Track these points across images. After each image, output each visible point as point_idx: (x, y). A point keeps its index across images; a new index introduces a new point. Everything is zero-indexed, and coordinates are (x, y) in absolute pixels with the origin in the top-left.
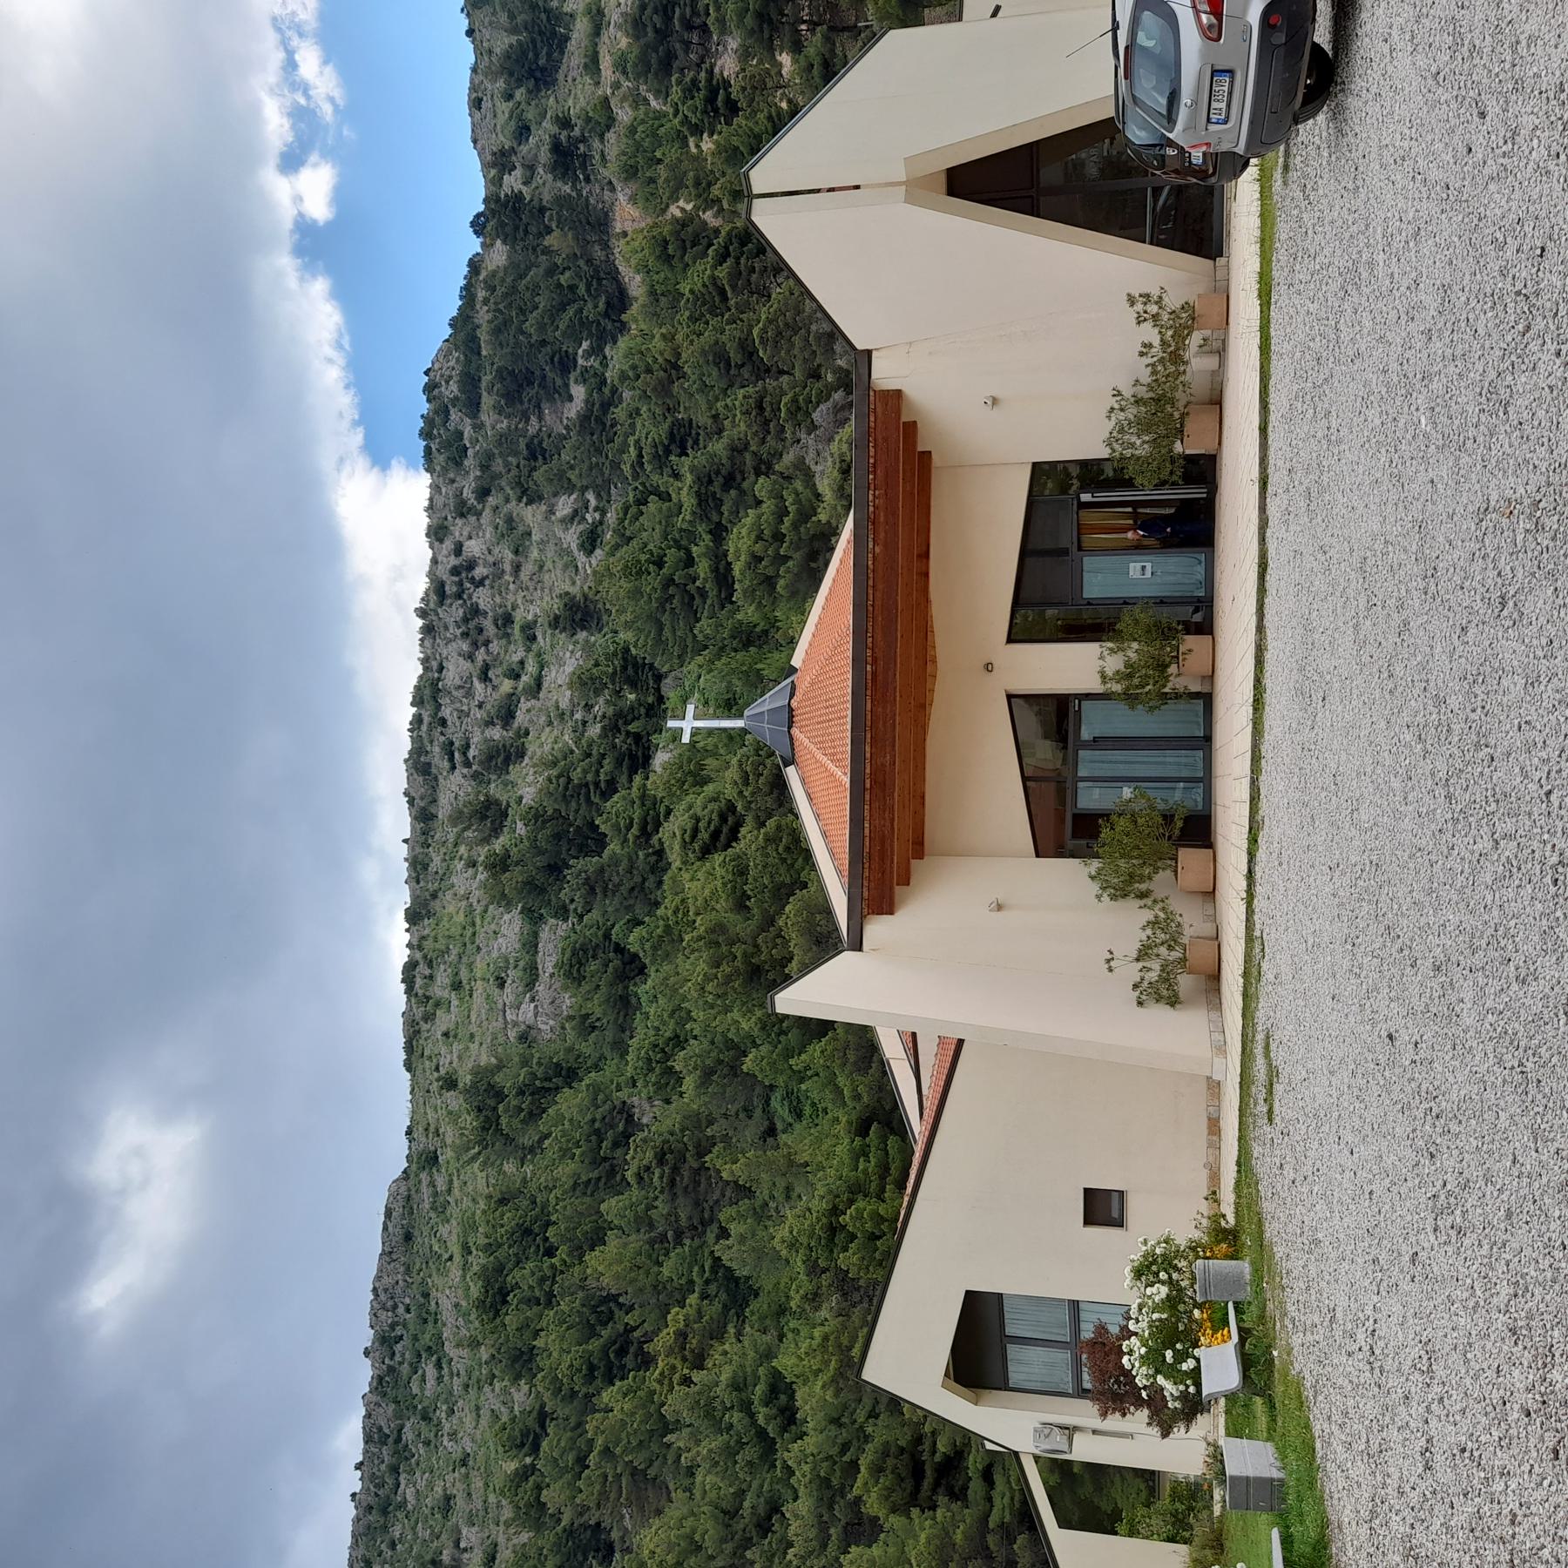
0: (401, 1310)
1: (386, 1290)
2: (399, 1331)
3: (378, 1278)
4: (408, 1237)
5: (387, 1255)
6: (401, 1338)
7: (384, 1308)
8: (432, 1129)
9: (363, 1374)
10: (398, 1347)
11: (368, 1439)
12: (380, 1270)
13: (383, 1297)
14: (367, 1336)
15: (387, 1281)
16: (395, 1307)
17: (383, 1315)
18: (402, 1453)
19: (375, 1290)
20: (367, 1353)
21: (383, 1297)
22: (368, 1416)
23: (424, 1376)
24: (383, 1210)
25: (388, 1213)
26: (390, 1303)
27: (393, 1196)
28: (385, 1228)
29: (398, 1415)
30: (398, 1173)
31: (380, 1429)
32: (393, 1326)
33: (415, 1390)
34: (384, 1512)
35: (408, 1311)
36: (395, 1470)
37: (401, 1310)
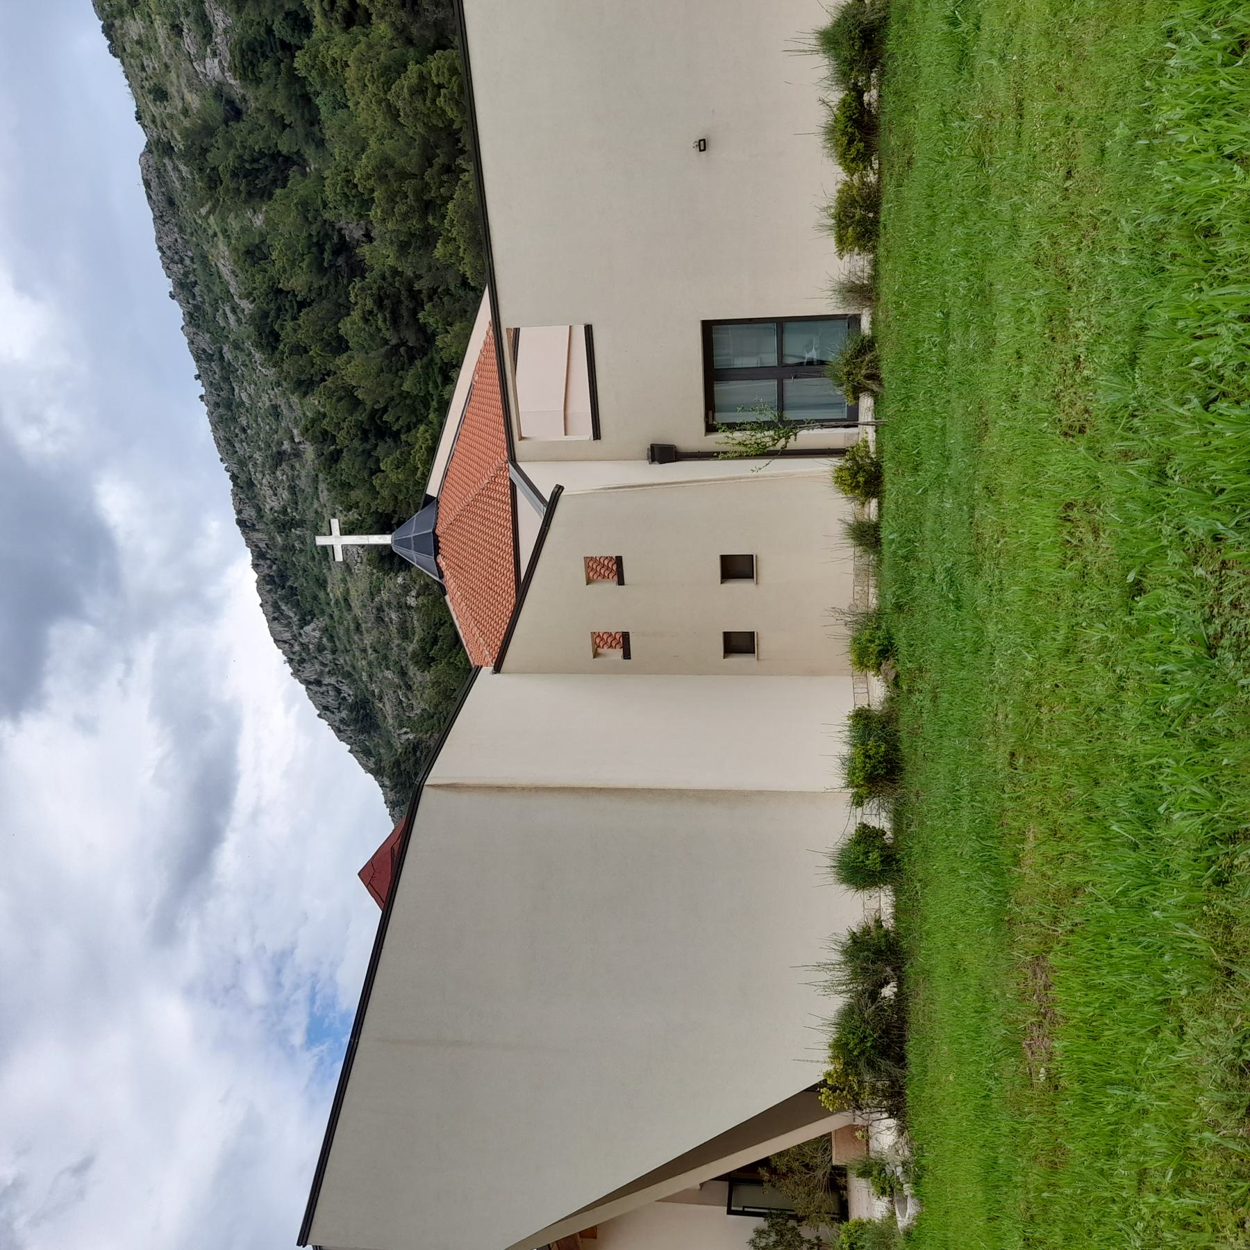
0: (187, 262)
1: (169, 248)
2: (192, 278)
3: (159, 239)
4: (171, 202)
5: (159, 218)
6: (196, 283)
7: (173, 261)
8: (158, 120)
9: (175, 313)
10: (197, 290)
11: (198, 359)
12: (158, 232)
13: (168, 253)
14: (168, 285)
15: (168, 240)
16: (182, 261)
17: (175, 268)
18: (228, 371)
19: (160, 248)
20: (172, 297)
21: (168, 253)
22: (191, 342)
23: (225, 313)
24: (141, 182)
25: (147, 184)
26: (176, 257)
27: (146, 169)
28: (149, 197)
29: (215, 341)
30: (142, 148)
31: (204, 350)
32: (186, 275)
33: (222, 324)
34: (229, 407)
35: (192, 259)
36: (226, 379)
37: (187, 262)
